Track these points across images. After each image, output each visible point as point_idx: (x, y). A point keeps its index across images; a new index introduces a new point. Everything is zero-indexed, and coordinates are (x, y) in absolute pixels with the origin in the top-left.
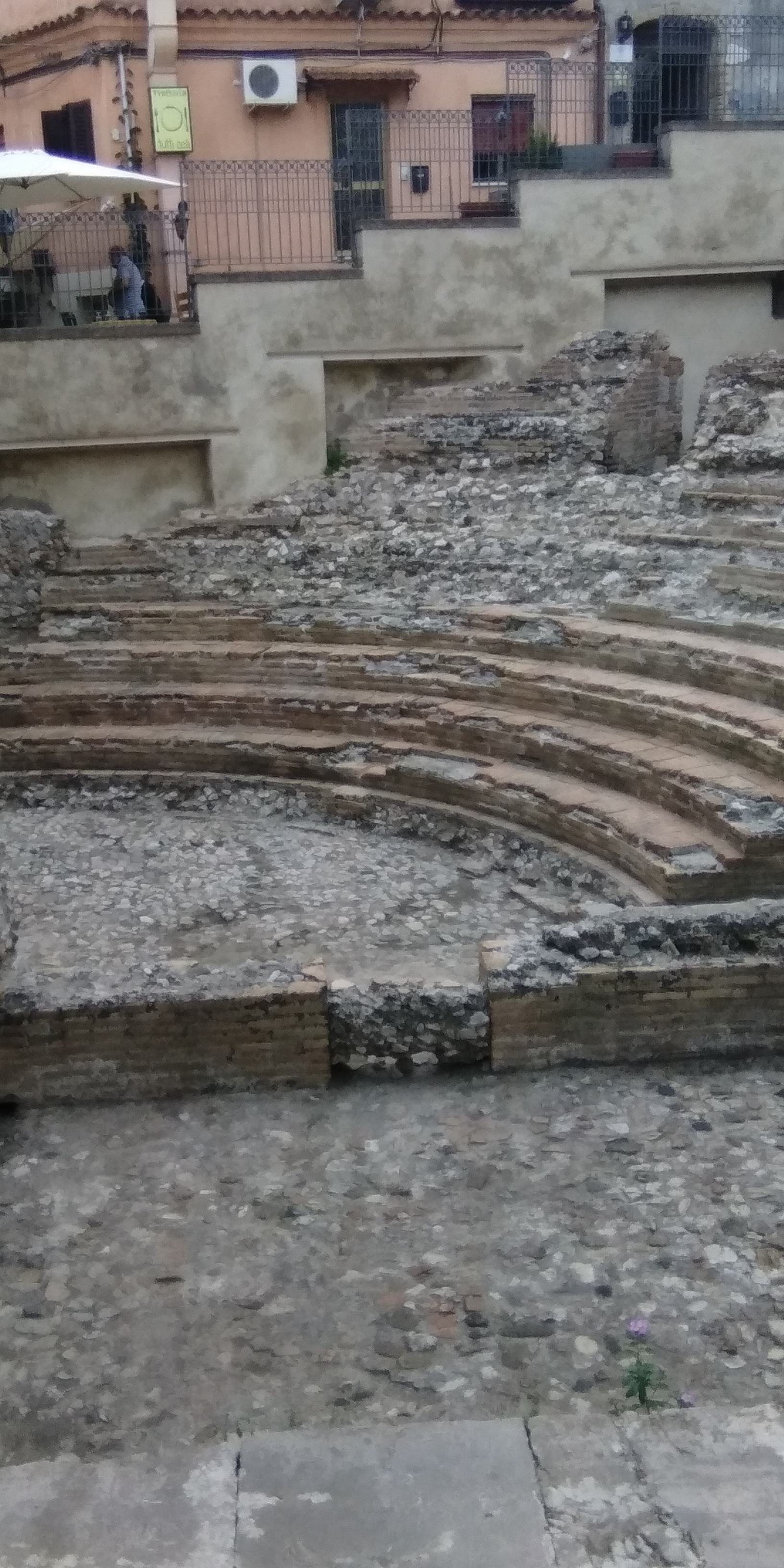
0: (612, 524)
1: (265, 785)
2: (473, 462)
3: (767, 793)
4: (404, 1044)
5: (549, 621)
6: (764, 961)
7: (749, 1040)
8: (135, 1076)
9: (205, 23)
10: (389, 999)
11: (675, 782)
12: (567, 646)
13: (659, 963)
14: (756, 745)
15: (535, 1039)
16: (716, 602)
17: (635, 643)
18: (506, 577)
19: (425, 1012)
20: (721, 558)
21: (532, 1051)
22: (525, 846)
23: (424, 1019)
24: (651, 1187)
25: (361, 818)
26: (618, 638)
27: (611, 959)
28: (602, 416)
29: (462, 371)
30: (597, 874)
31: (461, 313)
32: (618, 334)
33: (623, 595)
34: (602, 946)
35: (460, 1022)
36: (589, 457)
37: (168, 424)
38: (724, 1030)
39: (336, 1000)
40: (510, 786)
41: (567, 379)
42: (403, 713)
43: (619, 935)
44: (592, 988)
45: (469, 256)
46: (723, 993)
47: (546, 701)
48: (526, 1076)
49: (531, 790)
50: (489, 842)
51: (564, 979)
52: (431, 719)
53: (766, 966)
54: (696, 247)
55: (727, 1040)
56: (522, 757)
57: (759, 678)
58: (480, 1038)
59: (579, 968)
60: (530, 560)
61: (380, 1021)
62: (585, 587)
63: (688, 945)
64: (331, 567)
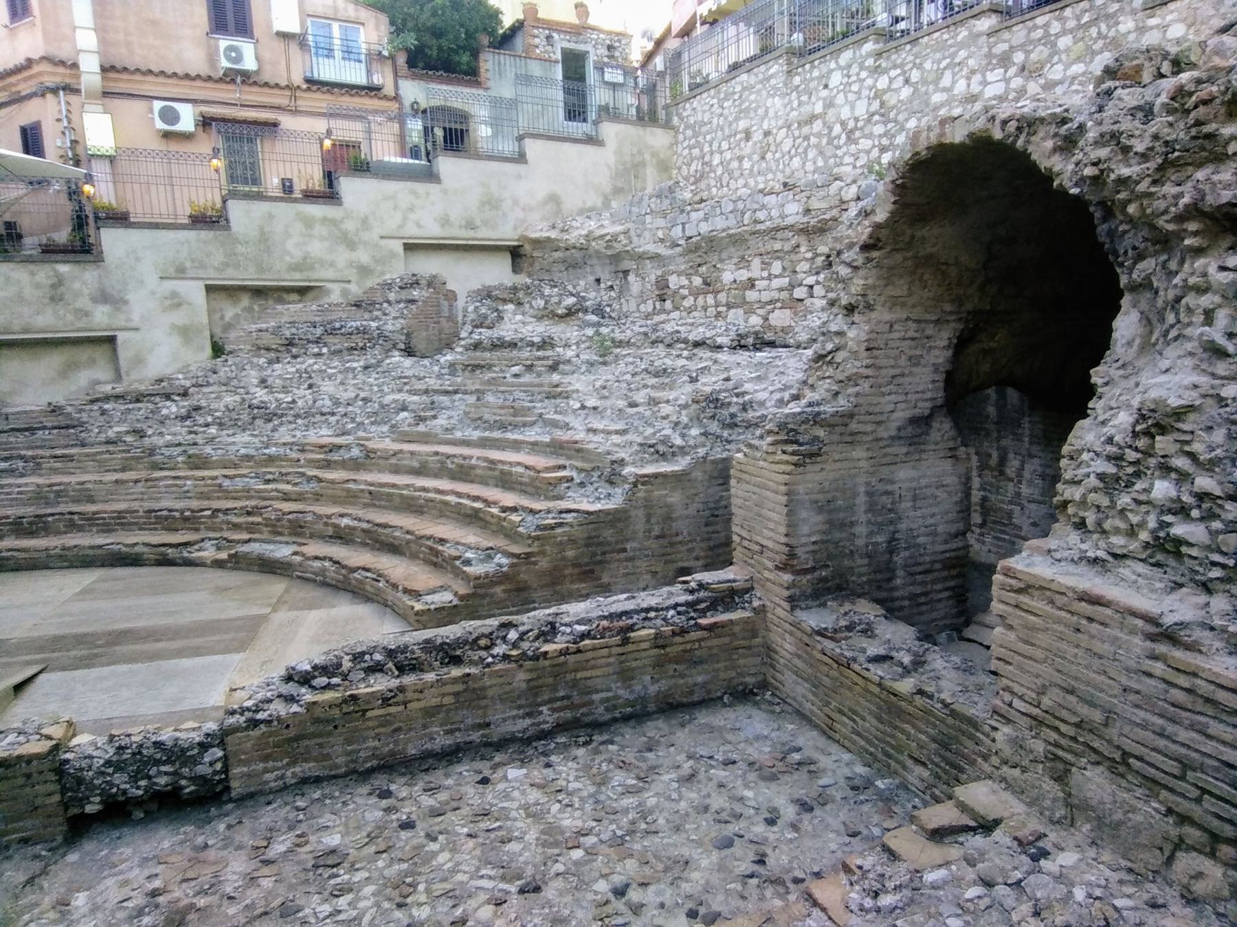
0: (405, 384)
2: (316, 350)
3: (490, 545)
4: (138, 788)
5: (358, 445)
6: (467, 671)
7: (460, 738)
9: (125, 76)
10: (121, 749)
11: (429, 543)
12: (369, 459)
13: (381, 684)
14: (484, 512)
15: (271, 764)
16: (469, 426)
17: (412, 453)
18: (332, 419)
19: (158, 756)
20: (472, 399)
21: (268, 776)
23: (158, 763)
24: (343, 902)
26: (401, 451)
27: (339, 685)
28: (402, 321)
29: (311, 295)
31: (305, 258)
32: (414, 275)
33: (409, 425)
35: (194, 761)
36: (394, 346)
37: (81, 325)
38: (437, 732)
39: (68, 756)
40: (317, 558)
41: (381, 300)
42: (249, 514)
43: (347, 664)
44: (318, 712)
45: (309, 223)
46: (435, 701)
47: (351, 497)
48: (263, 799)
49: (331, 559)
51: (295, 708)
53: (469, 675)
54: (460, 227)
55: (442, 741)
56: (331, 537)
57: (491, 469)
58: (215, 773)
59: (308, 696)
60: (350, 408)
61: (110, 770)
62: (385, 423)
64: (210, 419)
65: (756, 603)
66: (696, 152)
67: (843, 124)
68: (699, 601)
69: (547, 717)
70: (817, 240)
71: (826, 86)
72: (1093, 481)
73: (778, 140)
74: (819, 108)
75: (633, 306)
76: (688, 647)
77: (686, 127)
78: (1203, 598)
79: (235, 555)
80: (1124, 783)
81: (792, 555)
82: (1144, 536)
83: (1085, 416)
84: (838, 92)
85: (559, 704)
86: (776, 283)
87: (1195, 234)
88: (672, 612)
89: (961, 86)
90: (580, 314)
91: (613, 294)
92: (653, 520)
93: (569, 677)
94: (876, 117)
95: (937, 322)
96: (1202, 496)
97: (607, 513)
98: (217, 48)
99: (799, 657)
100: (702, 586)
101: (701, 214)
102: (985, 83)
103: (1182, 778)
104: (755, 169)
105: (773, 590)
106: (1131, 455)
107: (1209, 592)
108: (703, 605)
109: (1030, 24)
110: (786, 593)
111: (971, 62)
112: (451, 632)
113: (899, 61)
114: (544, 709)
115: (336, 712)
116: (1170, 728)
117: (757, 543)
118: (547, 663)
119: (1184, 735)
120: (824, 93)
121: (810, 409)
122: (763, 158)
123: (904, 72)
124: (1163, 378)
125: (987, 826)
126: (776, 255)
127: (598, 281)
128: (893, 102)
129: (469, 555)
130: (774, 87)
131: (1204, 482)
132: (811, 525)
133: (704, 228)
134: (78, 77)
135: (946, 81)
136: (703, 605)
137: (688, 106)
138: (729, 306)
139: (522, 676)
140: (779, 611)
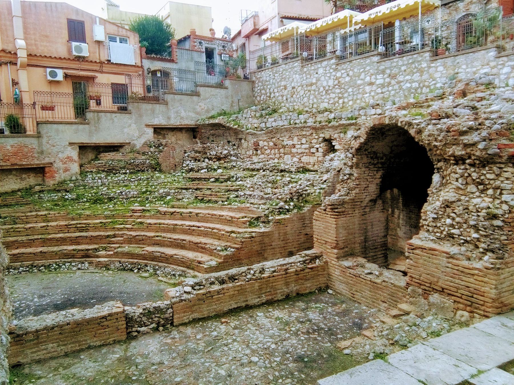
1: (74, 262)
2: (124, 171)
8: (62, 348)
9: (35, 58)
15: (185, 314)
22: (160, 267)
23: (154, 314)
25: (107, 267)
30: (183, 271)
34: (200, 286)
35: (165, 313)
39: (127, 312)
41: (148, 151)
43: (204, 282)
44: (200, 297)
50: (148, 268)
51: (192, 296)
52: (125, 237)
59: (195, 292)
61: (142, 316)
63: (222, 282)
65: (324, 260)
66: (263, 92)
67: (324, 87)
68: (307, 260)
69: (264, 299)
70: (320, 132)
71: (317, 73)
72: (431, 219)
73: (298, 91)
74: (314, 81)
75: (243, 152)
76: (305, 274)
77: (259, 82)
78: (459, 247)
79: (116, 252)
80: (443, 296)
81: (337, 244)
82: (445, 233)
83: (427, 202)
84: (322, 76)
85: (267, 294)
86: (304, 146)
87: (453, 160)
88: (299, 264)
89: (368, 79)
90: (229, 157)
91: (235, 147)
92: (281, 235)
93: (271, 284)
94: (337, 87)
95: (377, 170)
96: (458, 223)
97: (266, 232)
98: (71, 46)
99: (341, 276)
100: (307, 255)
101: (273, 119)
102: (376, 79)
103: (457, 292)
104: (289, 100)
105: (331, 255)
106: (441, 213)
107: (461, 246)
108: (308, 261)
109: (392, 61)
110: (336, 256)
111: (371, 71)
112: (222, 274)
113: (345, 68)
114: (263, 295)
115: (204, 296)
116: (454, 280)
117: (324, 240)
118: (264, 280)
119: (457, 281)
120: (316, 75)
121: (341, 198)
122: (292, 97)
123: (347, 72)
124: (447, 194)
125: (408, 313)
126: (304, 136)
127: (229, 142)
128: (343, 82)
129: (219, 248)
130: (296, 71)
131: (458, 219)
132: (343, 233)
133: (274, 124)
134: (17, 58)
135: (362, 76)
136: (308, 261)
137: (259, 74)
138: (285, 154)
139: (257, 284)
140: (333, 262)
